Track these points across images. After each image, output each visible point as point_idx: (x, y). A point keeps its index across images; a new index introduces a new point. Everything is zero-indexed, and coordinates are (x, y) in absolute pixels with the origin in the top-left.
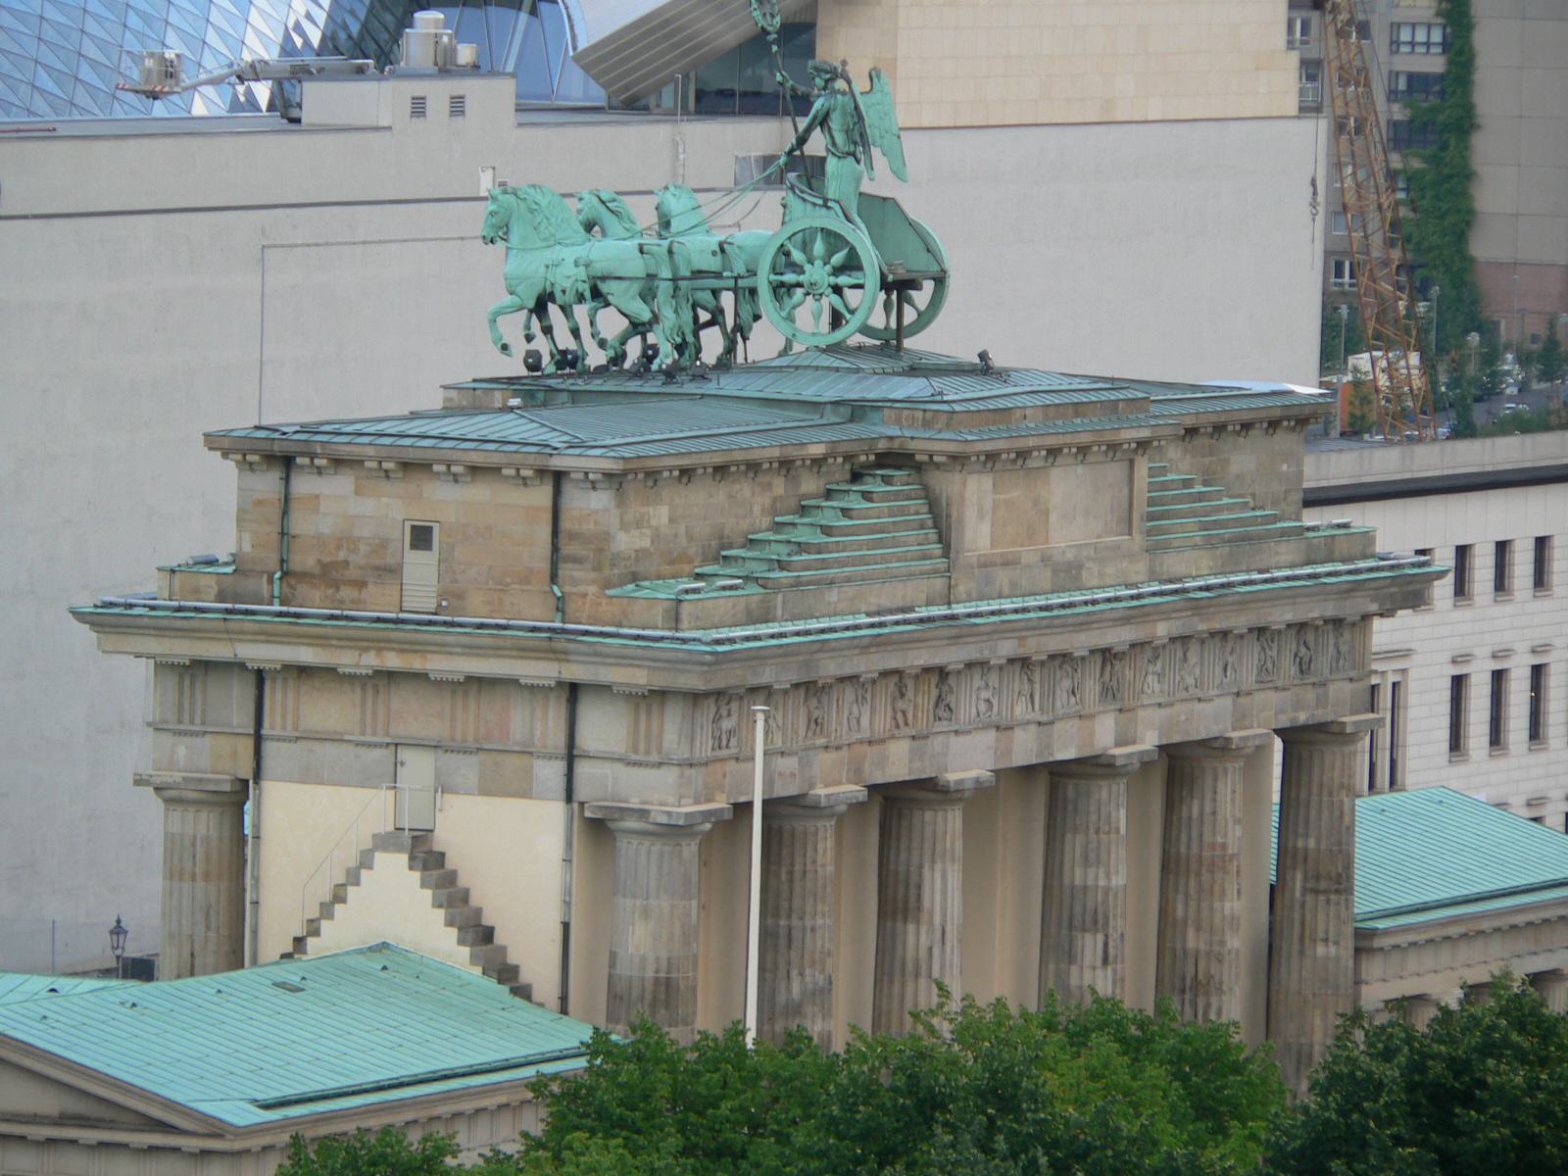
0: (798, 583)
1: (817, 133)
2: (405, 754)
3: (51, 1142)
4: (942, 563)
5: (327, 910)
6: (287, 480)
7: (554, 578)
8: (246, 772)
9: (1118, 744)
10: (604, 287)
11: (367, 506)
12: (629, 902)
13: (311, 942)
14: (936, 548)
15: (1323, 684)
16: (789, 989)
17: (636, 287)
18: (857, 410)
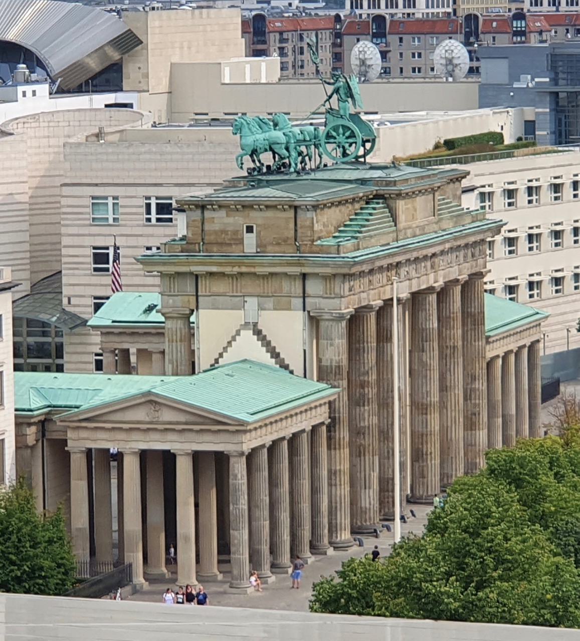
0: (365, 237)
1: (335, 94)
2: (246, 299)
3: (184, 430)
4: (394, 228)
5: (225, 349)
6: (203, 213)
7: (296, 240)
8: (193, 307)
9: (435, 282)
10: (273, 146)
11: (231, 220)
12: (325, 342)
13: (220, 360)
14: (393, 224)
15: (477, 260)
16: (364, 368)
17: (283, 146)
18: (363, 182)
